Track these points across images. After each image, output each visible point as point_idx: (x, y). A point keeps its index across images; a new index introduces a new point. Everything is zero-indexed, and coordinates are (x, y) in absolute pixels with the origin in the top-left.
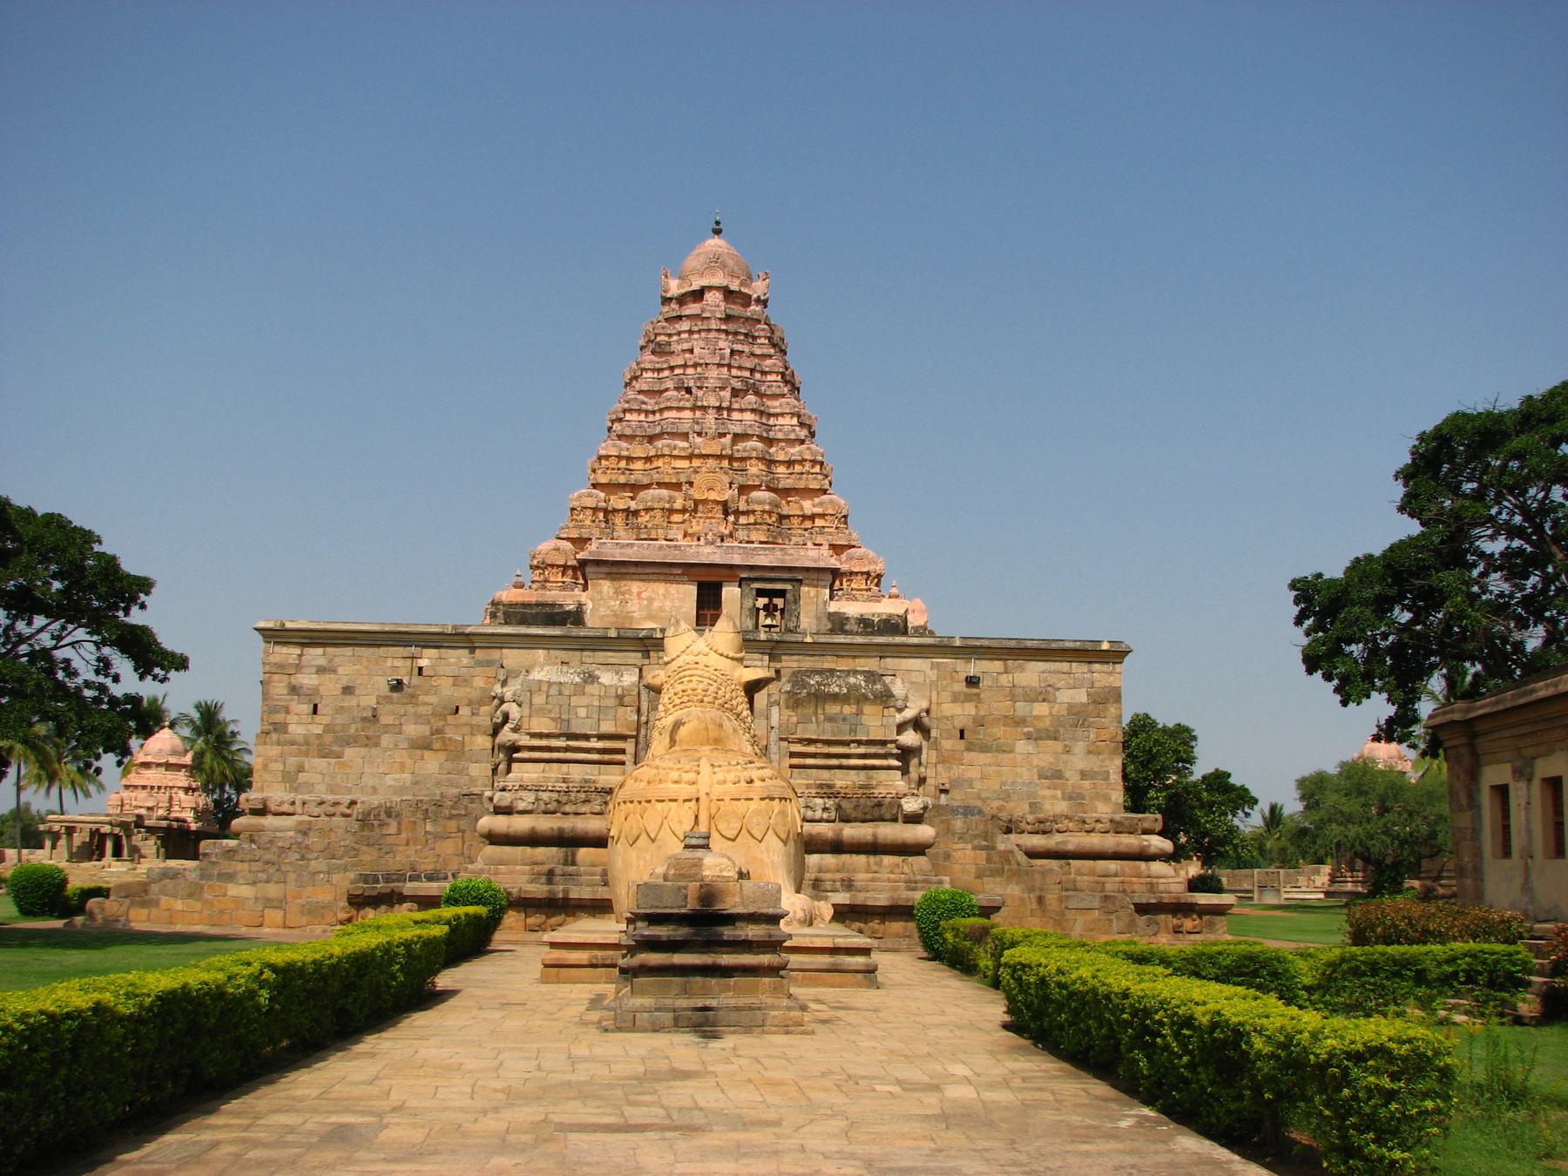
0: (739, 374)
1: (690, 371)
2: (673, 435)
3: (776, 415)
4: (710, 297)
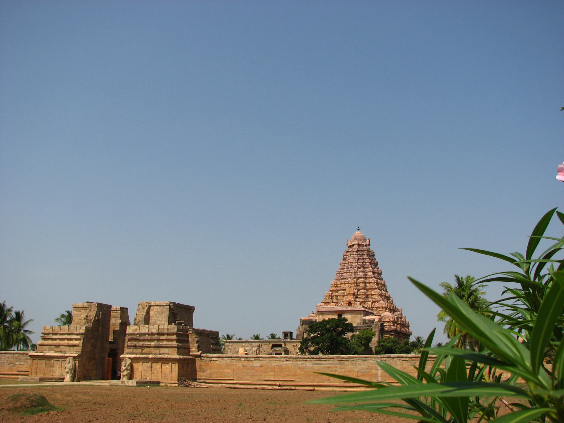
0: (360, 264)
1: (350, 264)
2: (346, 279)
3: (367, 272)
4: (356, 246)
